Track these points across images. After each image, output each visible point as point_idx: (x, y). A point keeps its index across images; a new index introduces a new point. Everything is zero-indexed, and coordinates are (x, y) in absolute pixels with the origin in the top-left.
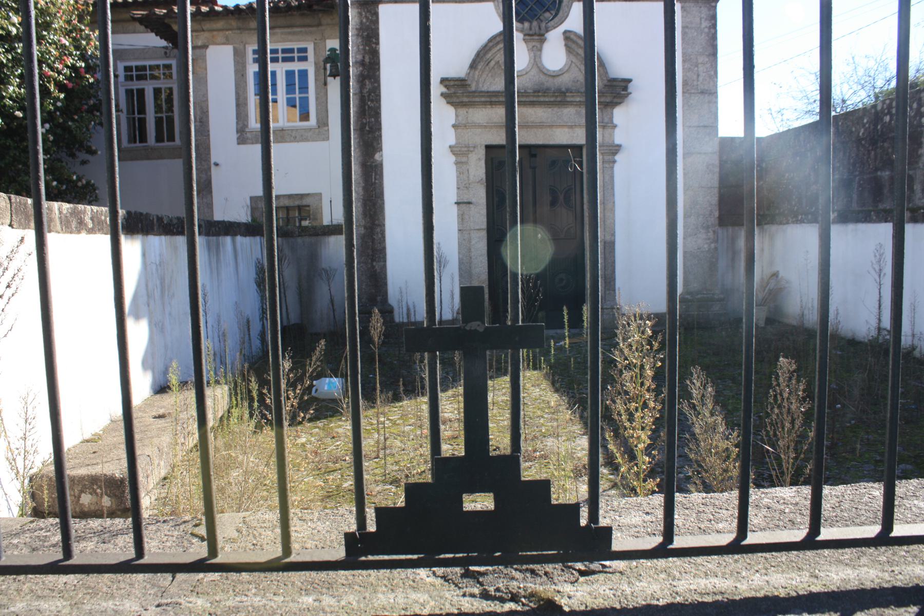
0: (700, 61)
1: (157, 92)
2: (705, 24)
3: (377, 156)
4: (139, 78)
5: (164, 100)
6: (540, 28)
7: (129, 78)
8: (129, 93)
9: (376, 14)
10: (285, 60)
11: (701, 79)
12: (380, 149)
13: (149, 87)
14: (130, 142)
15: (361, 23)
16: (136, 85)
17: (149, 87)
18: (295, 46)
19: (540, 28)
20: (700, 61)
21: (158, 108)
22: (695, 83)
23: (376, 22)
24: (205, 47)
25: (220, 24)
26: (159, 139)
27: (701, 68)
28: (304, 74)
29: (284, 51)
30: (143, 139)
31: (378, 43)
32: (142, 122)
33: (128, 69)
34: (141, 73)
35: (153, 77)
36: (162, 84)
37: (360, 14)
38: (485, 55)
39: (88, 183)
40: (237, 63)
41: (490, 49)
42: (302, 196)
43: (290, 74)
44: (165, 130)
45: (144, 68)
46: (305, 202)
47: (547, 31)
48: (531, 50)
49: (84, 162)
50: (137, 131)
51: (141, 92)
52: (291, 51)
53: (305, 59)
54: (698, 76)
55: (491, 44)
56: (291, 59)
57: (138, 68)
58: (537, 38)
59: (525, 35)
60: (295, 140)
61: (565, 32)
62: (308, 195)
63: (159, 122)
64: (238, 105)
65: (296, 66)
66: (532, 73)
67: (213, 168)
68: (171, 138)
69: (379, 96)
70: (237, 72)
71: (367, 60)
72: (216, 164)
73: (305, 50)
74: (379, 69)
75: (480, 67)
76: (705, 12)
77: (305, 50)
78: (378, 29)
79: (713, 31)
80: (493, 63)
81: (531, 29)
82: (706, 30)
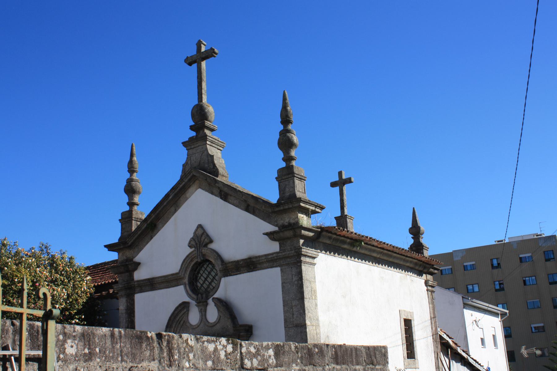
0: (293, 304)
2: (295, 279)
6: (202, 298)
9: (133, 300)
11: (295, 316)
15: (127, 306)
19: (202, 298)
20: (293, 304)
22: (292, 320)
27: (294, 310)
31: (134, 316)
37: (127, 300)
38: (175, 318)
41: (177, 315)
47: (208, 298)
48: (201, 311)
54: (293, 314)
55: (176, 312)
58: (202, 304)
59: (198, 303)
61: (213, 298)
66: (201, 326)
75: (174, 326)
76: (294, 270)
78: (134, 308)
79: (300, 282)
80: (182, 322)
81: (197, 299)
82: (296, 282)
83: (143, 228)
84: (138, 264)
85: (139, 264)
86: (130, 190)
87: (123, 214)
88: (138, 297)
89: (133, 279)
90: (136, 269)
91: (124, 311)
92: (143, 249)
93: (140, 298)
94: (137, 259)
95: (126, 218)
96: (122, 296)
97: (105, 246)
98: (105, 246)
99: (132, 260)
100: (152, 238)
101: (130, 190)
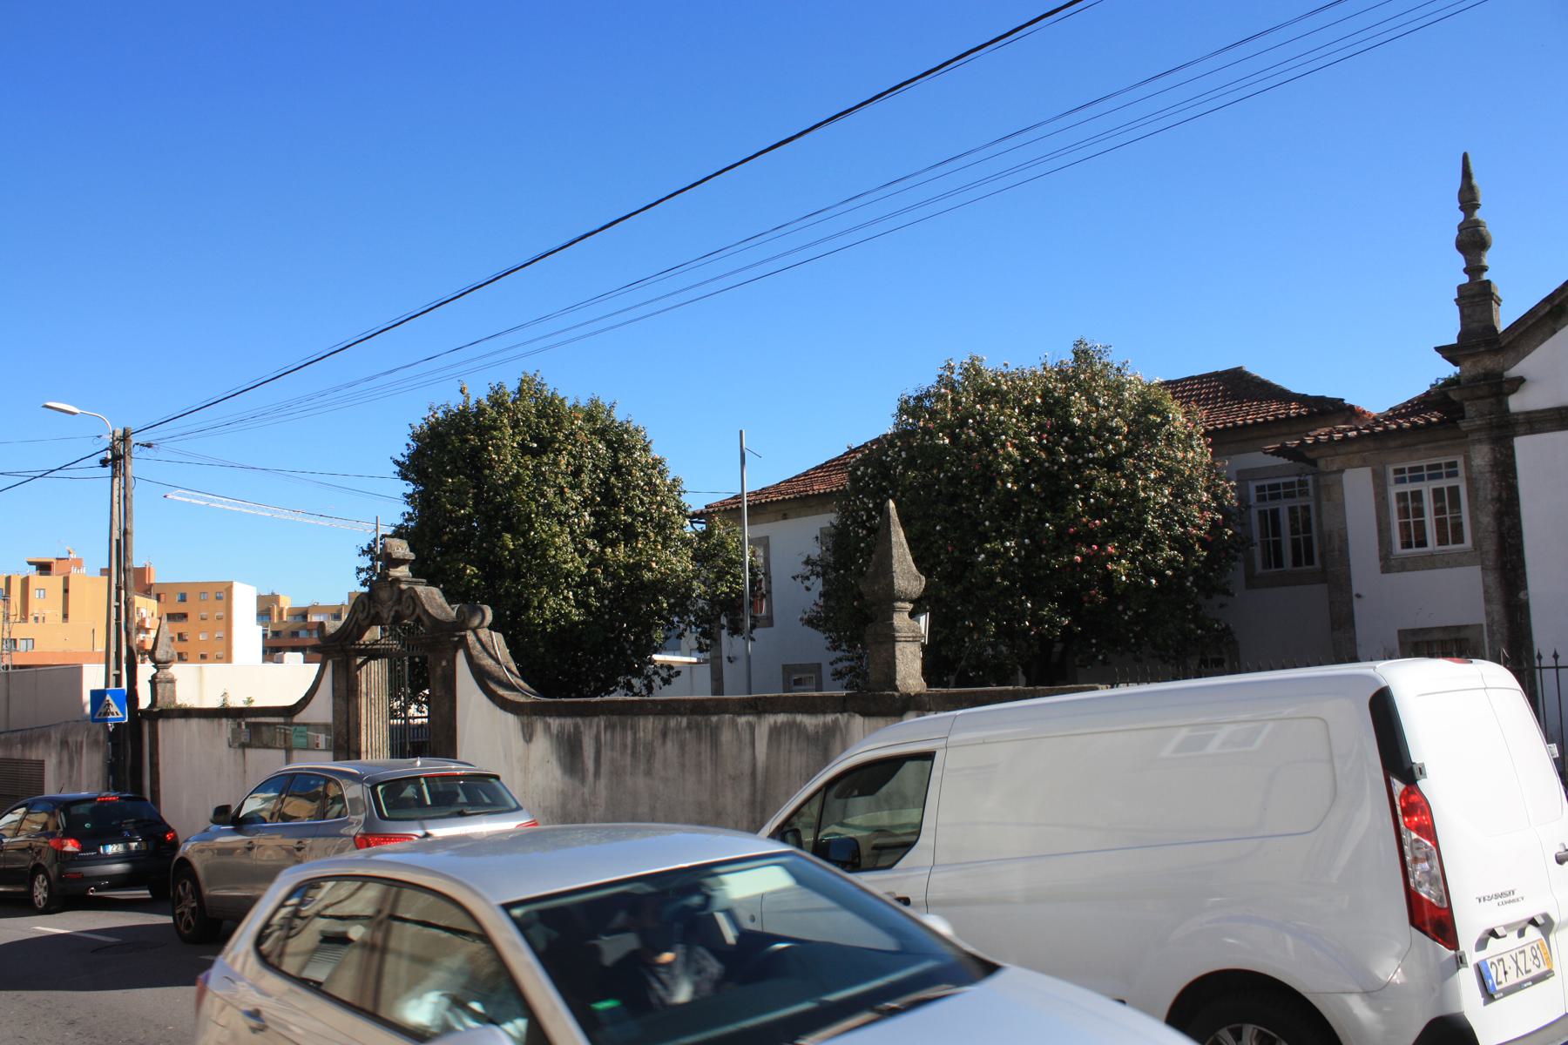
1: (1292, 510)
3: (1521, 595)
4: (1273, 497)
5: (1302, 522)
7: (1261, 498)
8: (1262, 514)
9: (1512, 448)
10: (1431, 477)
12: (1526, 588)
13: (1283, 506)
14: (1264, 567)
16: (1269, 506)
17: (1283, 506)
18: (1443, 461)
21: (1294, 531)
23: (1512, 456)
24: (1342, 471)
25: (1356, 447)
26: (1296, 562)
28: (1454, 491)
29: (1430, 467)
30: (1279, 563)
31: (1515, 477)
32: (1277, 545)
33: (1260, 489)
34: (1274, 492)
35: (1287, 496)
36: (1298, 502)
39: (1227, 627)
40: (1376, 486)
42: (1459, 628)
43: (1438, 494)
44: (1303, 553)
45: (1277, 486)
46: (1462, 635)
49: (1222, 606)
50: (1273, 555)
51: (1275, 513)
52: (1439, 466)
53: (1455, 474)
56: (1439, 476)
57: (1271, 487)
60: (1448, 565)
62: (1466, 627)
63: (1295, 545)
64: (1380, 531)
65: (1444, 483)
67: (1355, 600)
68: (1310, 561)
69: (1520, 532)
70: (1376, 495)
71: (1504, 495)
72: (1359, 596)
73: (1454, 464)
74: (1518, 505)
77: (1454, 464)
83: (1542, 313)
84: (1520, 382)
85: (1520, 382)
86: (1472, 242)
87: (1460, 288)
88: (1526, 448)
89: (1507, 410)
90: (1514, 391)
91: (1488, 468)
92: (1529, 352)
93: (1526, 448)
94: (1514, 372)
95: (1476, 297)
96: (1479, 441)
97: (1437, 349)
98: (1437, 349)
99: (1501, 375)
100: (1554, 332)
101: (1472, 242)
